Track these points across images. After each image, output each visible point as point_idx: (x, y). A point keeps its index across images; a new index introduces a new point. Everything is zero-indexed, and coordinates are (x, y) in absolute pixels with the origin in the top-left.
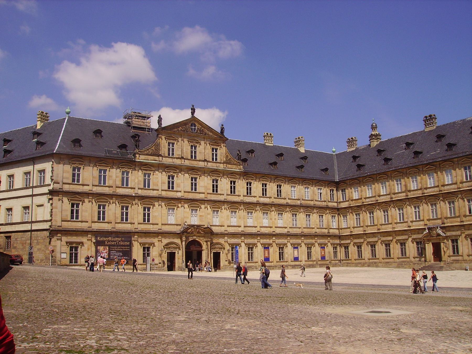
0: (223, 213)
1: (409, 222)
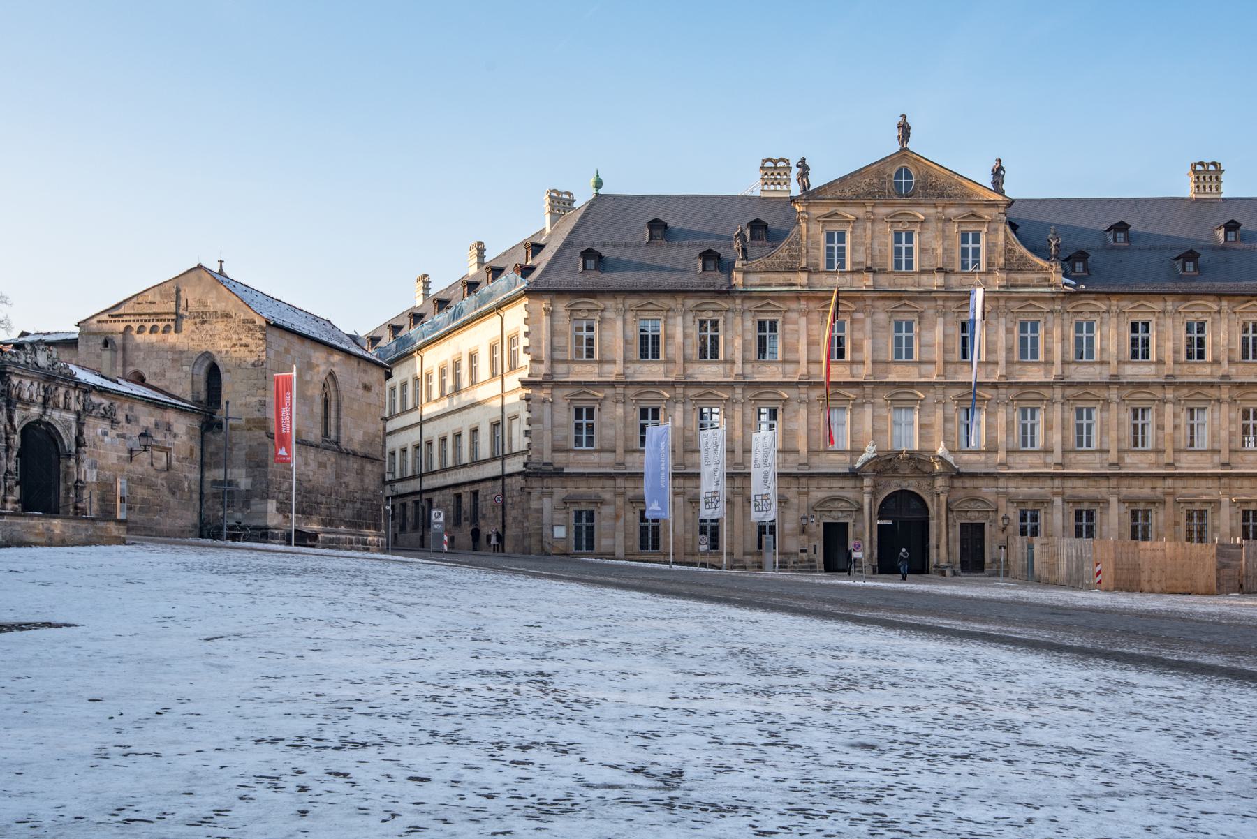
0: (995, 414)
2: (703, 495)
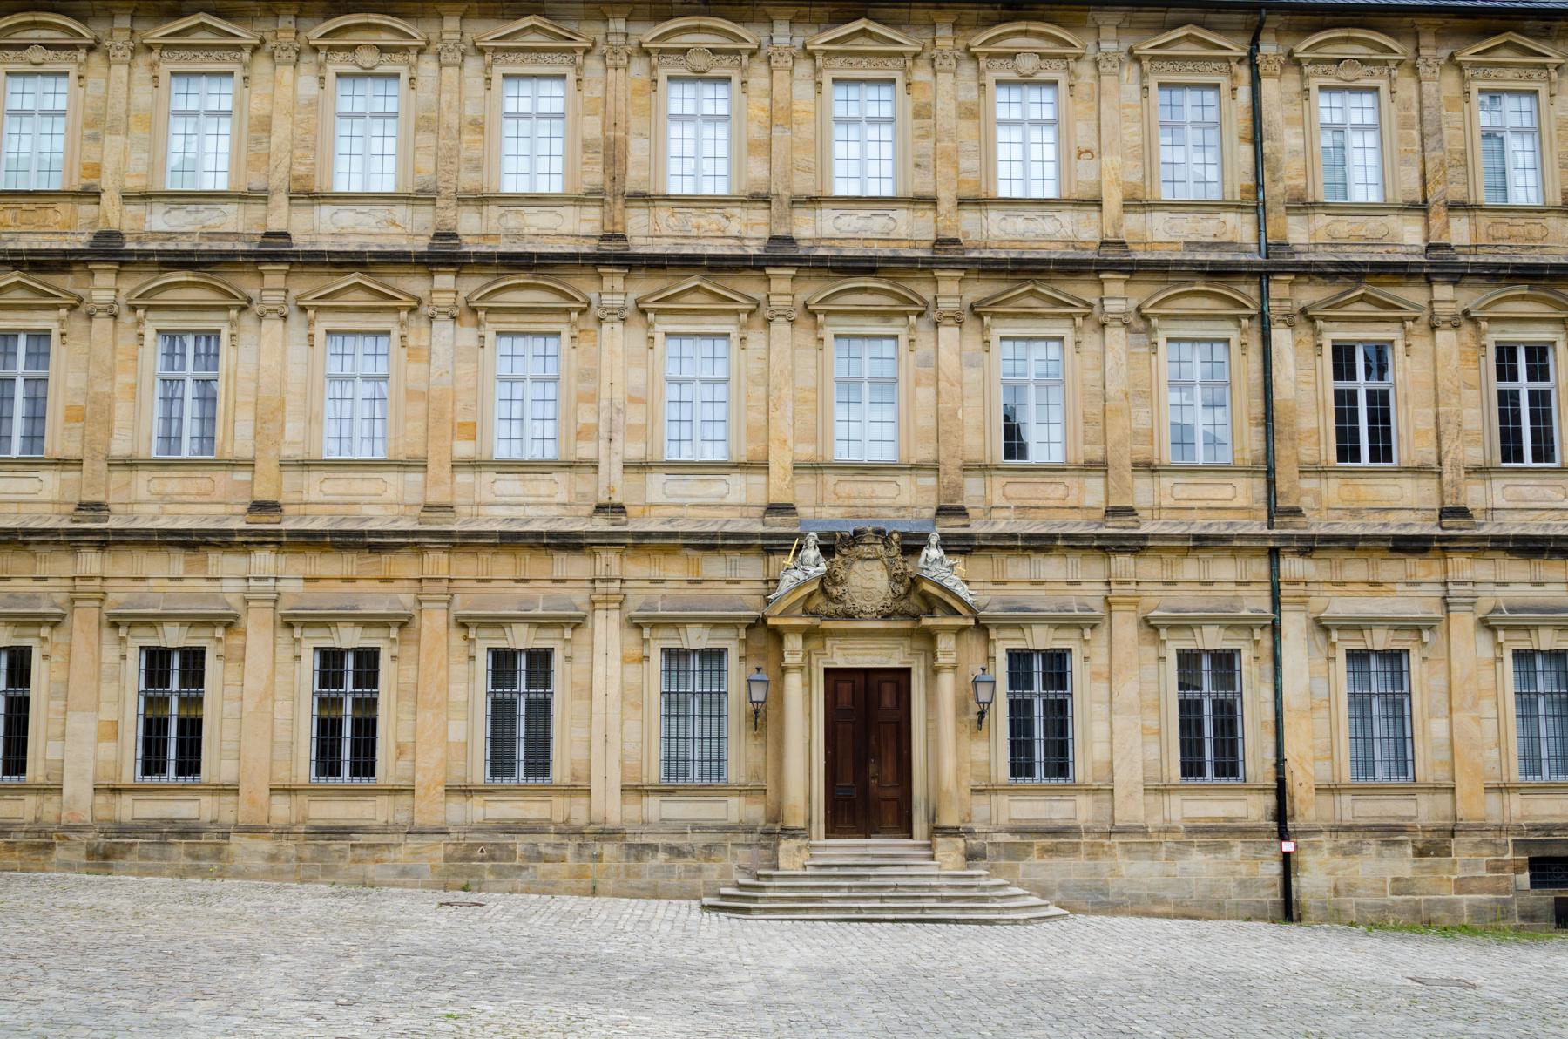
1: (612, 472)
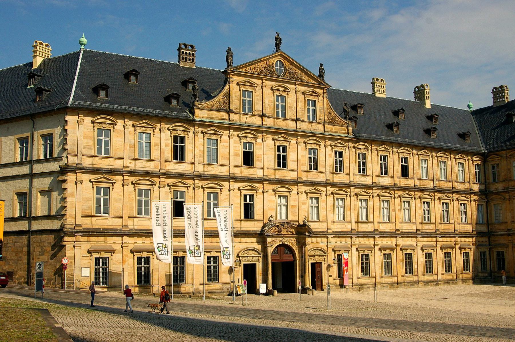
2: (155, 246)
